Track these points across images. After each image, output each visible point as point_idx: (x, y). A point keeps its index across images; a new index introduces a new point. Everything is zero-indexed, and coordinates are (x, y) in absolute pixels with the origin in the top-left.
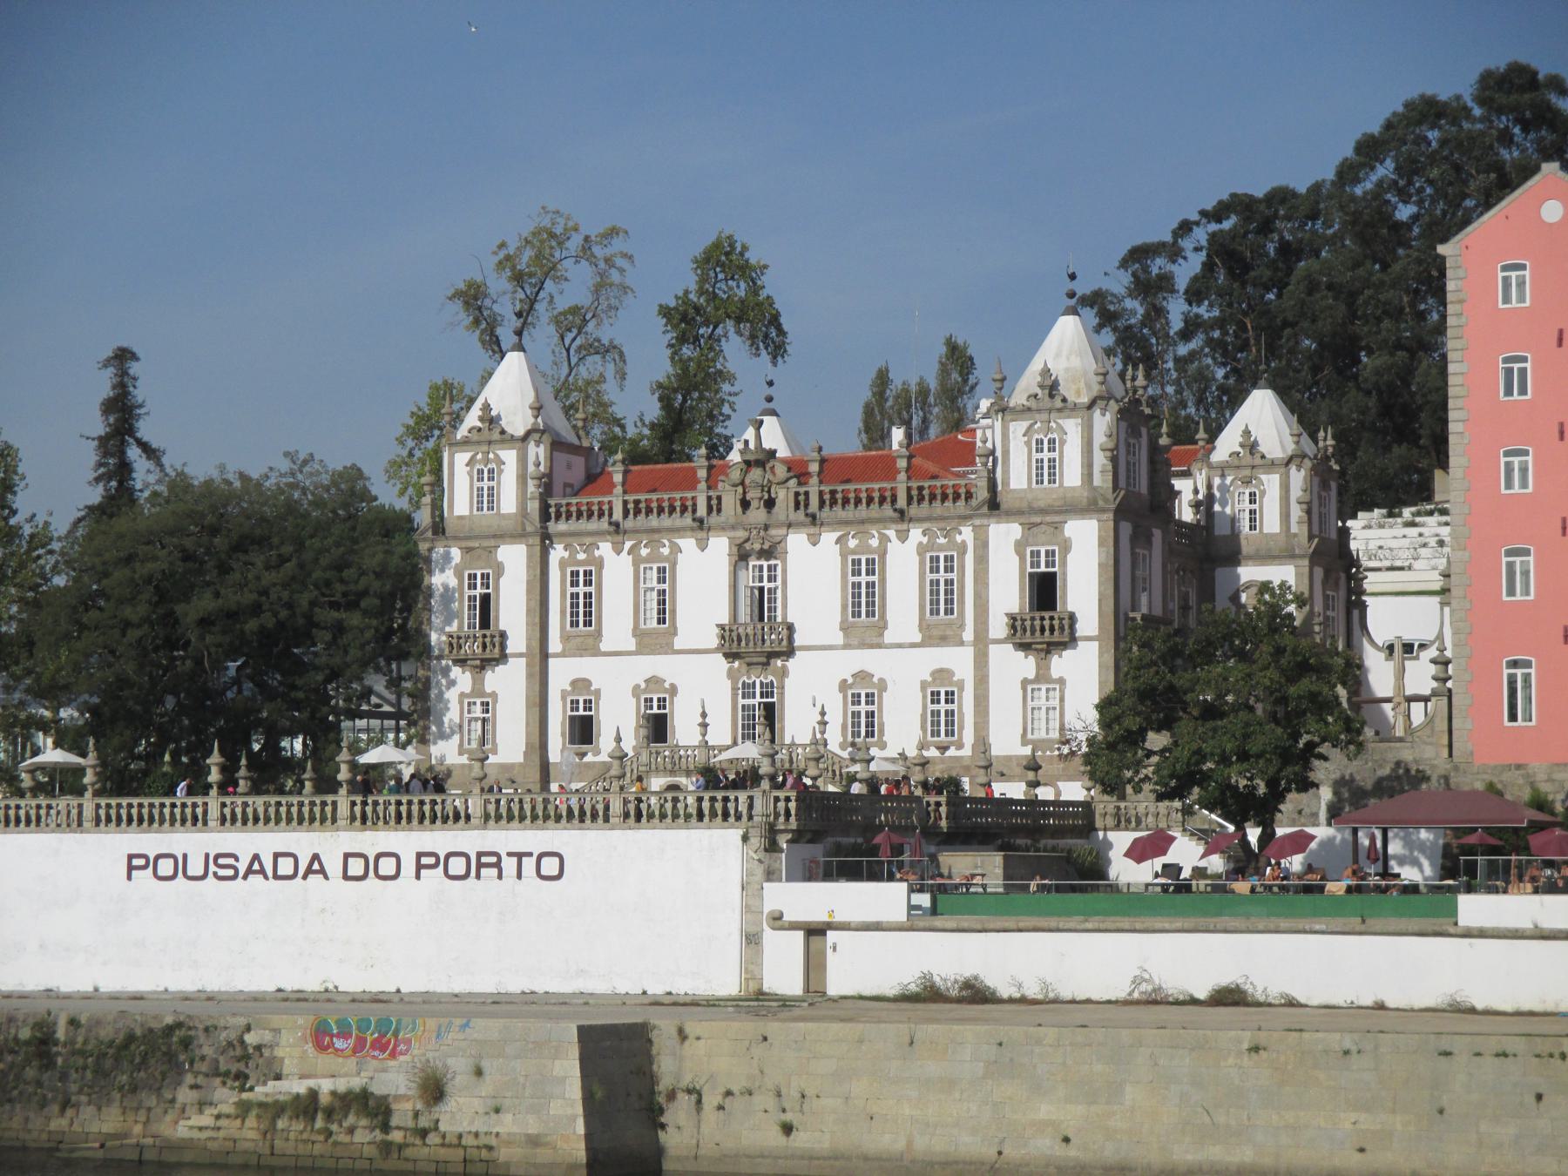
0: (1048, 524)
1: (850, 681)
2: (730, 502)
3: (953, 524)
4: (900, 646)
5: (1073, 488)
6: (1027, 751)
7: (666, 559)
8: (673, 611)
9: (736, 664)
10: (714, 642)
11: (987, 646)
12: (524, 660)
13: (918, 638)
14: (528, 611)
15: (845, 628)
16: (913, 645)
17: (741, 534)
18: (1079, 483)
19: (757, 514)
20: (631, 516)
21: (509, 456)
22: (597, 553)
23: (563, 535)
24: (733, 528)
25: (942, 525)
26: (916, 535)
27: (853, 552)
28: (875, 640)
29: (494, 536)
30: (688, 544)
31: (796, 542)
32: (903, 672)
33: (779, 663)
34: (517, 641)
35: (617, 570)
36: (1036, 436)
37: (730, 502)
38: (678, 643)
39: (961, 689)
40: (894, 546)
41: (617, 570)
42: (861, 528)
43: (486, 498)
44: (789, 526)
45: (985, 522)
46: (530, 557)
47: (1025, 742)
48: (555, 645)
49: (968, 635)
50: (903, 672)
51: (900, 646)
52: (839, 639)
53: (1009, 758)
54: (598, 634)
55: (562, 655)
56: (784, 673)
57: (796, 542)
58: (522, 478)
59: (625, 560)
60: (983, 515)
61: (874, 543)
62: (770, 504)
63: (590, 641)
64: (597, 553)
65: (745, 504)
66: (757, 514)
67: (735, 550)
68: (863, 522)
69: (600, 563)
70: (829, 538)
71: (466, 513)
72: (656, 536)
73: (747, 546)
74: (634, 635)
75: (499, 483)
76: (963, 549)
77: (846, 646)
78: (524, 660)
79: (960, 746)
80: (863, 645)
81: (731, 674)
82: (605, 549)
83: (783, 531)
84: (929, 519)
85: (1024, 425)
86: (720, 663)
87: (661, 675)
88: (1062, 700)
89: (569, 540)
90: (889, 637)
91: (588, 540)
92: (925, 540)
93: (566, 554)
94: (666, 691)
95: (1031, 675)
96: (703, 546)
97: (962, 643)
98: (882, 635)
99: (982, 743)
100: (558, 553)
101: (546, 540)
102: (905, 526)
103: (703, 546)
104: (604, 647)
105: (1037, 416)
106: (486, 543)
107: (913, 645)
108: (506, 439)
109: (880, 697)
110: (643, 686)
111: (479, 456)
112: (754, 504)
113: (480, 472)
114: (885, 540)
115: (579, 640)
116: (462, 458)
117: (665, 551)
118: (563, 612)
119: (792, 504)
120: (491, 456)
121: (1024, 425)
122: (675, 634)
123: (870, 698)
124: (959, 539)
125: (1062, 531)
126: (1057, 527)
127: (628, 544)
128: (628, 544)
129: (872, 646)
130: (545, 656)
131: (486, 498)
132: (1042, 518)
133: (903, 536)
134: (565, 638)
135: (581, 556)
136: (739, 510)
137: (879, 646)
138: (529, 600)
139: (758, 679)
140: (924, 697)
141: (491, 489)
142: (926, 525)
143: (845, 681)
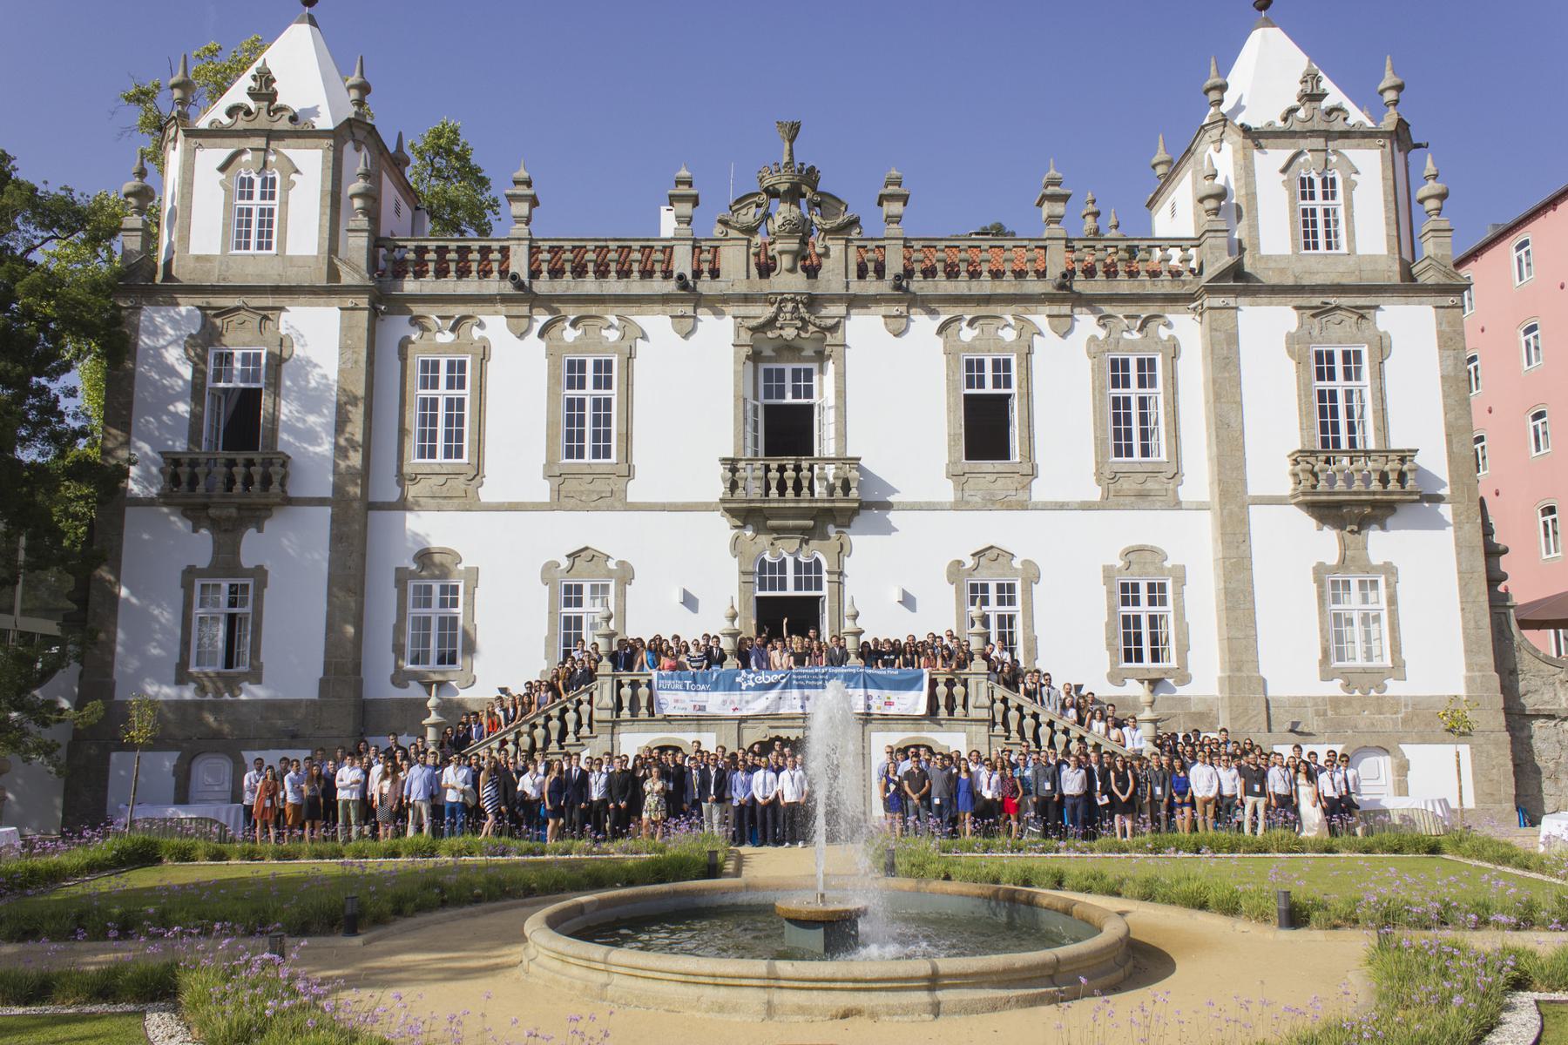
2: (734, 259)
3: (1152, 309)
4: (1062, 506)
5: (1373, 258)
6: (1335, 688)
7: (615, 348)
8: (627, 437)
11: (1244, 507)
12: (328, 510)
13: (1096, 494)
16: (1086, 506)
21: (310, 161)
24: (746, 299)
25: (1132, 309)
29: (276, 290)
30: (656, 323)
35: (516, 370)
37: (734, 259)
39: (1181, 581)
43: (252, 226)
45: (1231, 301)
46: (346, 330)
47: (1327, 674)
51: (1062, 506)
52: (946, 491)
53: (1299, 703)
57: (864, 330)
61: (1009, 335)
70: (923, 325)
71: (215, 249)
75: (285, 203)
76: (1174, 353)
77: (960, 505)
82: (494, 326)
86: (721, 527)
88: (1392, 600)
90: (1040, 491)
91: (458, 311)
92: (1102, 334)
95: (1333, 559)
97: (1177, 505)
98: (1027, 487)
104: (487, 494)
107: (1086, 506)
108: (300, 130)
109: (1028, 592)
111: (247, 157)
114: (1027, 332)
116: (211, 157)
122: (629, 474)
123: (1006, 594)
129: (1009, 507)
131: (252, 226)
132: (1331, 298)
137: (1023, 506)
141: (266, 213)
143: (960, 563)
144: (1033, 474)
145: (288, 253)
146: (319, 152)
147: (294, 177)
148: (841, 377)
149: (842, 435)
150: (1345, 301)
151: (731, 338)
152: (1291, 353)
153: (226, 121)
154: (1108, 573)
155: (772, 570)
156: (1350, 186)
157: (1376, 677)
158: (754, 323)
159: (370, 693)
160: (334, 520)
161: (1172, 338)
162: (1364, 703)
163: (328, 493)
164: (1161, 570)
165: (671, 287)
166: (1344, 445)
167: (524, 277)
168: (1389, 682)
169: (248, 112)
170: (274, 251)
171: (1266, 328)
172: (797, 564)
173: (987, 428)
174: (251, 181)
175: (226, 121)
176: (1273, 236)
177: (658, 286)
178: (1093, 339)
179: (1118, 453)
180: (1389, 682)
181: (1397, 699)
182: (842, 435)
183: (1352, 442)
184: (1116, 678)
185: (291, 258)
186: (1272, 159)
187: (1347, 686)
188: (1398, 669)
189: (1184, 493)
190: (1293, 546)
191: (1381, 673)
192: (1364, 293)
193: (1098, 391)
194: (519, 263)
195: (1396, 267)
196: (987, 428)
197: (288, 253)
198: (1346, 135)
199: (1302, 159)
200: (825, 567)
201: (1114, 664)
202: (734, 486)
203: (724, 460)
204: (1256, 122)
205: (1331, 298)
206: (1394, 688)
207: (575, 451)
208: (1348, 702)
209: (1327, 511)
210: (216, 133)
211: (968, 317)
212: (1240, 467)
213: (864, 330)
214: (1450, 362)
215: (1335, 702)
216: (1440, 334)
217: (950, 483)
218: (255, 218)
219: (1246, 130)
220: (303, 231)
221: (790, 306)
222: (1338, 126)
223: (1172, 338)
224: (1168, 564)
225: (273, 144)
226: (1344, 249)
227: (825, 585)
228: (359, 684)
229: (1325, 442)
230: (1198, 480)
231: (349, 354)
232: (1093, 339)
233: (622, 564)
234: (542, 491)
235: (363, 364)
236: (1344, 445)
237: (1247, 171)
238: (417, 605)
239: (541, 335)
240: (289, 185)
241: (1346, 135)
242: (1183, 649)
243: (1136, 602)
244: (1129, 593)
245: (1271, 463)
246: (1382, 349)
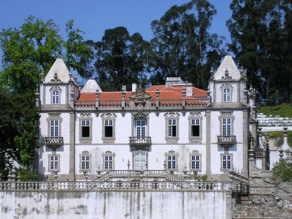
5: (235, 103)
10: (128, 142)
18: (237, 101)
27: (169, 118)
30: (119, 115)
31: (152, 116)
40: (181, 117)
48: (77, 141)
49: (204, 141)
53: (217, 175)
57: (152, 116)
58: (67, 94)
70: (162, 114)
77: (166, 144)
97: (201, 144)
98: (177, 141)
104: (92, 142)
123: (174, 158)
125: (232, 114)
129: (174, 144)
134: (81, 140)
137: (177, 144)
140: (190, 158)
145: (61, 104)
156: (232, 91)
158: (134, 114)
170: (59, 103)
173: (173, 131)
182: (148, 133)
189: (202, 142)
192: (231, 110)
196: (173, 131)
197: (61, 104)
208: (224, 175)
214: (245, 121)
215: (222, 175)
220: (63, 100)
224: (199, 153)
225: (57, 86)
239: (101, 117)
241: (232, 82)
242: (201, 167)
244: (193, 158)
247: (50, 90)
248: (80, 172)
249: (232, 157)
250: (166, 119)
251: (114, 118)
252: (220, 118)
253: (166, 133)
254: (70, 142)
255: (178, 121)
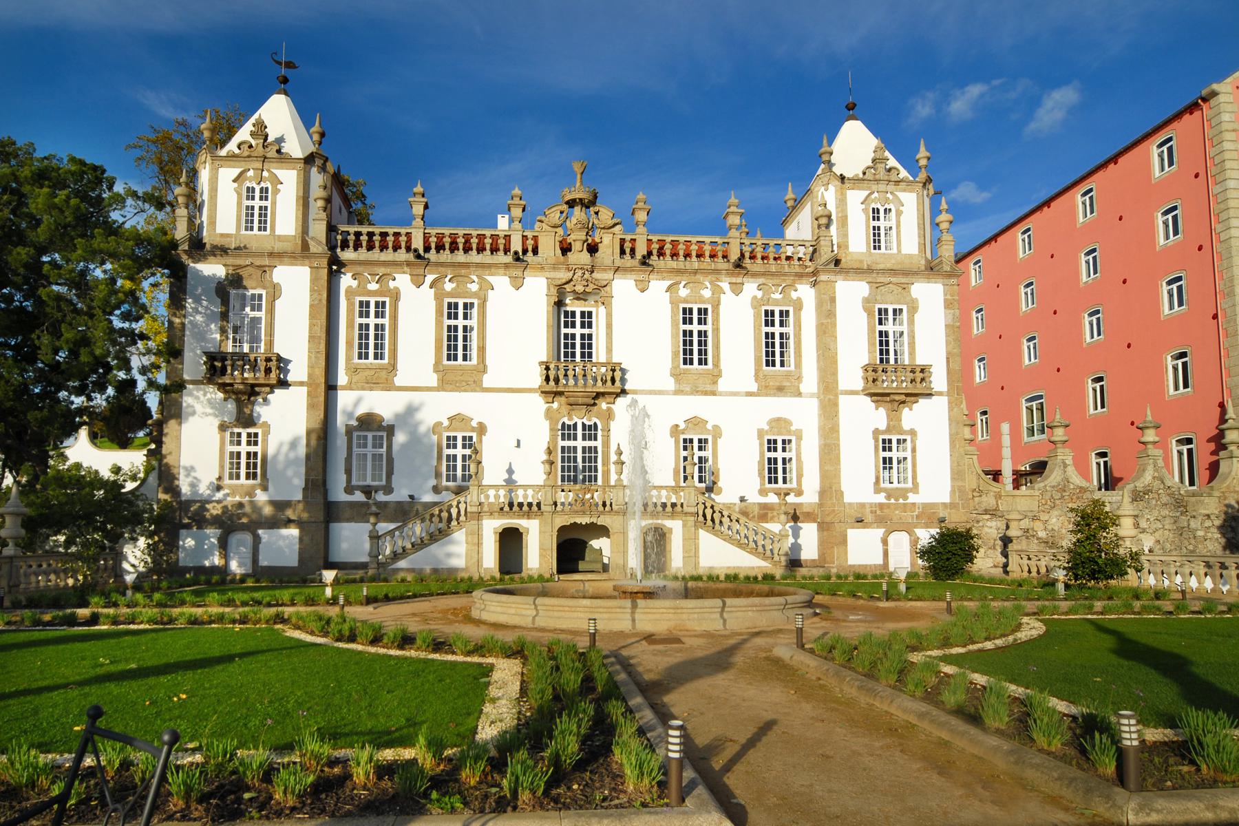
0: (897, 284)
1: (682, 426)
3: (789, 280)
5: (911, 256)
6: (881, 498)
7: (475, 295)
8: (482, 349)
9: (555, 405)
11: (836, 396)
12: (305, 389)
13: (754, 387)
14: (312, 338)
15: (676, 375)
16: (749, 394)
17: (563, 275)
18: (916, 252)
19: (579, 256)
20: (433, 251)
21: (289, 178)
22: (392, 284)
23: (353, 262)
24: (555, 267)
25: (776, 281)
26: (751, 288)
27: (685, 301)
28: (709, 388)
29: (271, 255)
30: (500, 282)
32: (738, 421)
33: (604, 406)
34: (298, 371)
35: (417, 307)
36: (873, 205)
37: (549, 247)
38: (488, 381)
39: (799, 438)
40: (727, 298)
41: (417, 307)
42: (693, 278)
44: (617, 270)
45: (833, 278)
46: (314, 281)
47: (878, 490)
50: (738, 421)
52: (670, 384)
53: (862, 505)
54: (393, 367)
55: (349, 387)
56: (610, 415)
57: (623, 288)
58: (305, 201)
59: (427, 293)
60: (829, 271)
61: (707, 293)
62: (593, 249)
63: (383, 374)
64: (392, 284)
65: (566, 249)
66: (579, 256)
67: (554, 291)
68: (695, 272)
69: (396, 296)
70: (658, 286)
71: (232, 230)
72: (463, 272)
73: (568, 288)
74: (436, 370)
75: (274, 203)
76: (799, 305)
78: (305, 389)
79: (799, 493)
80: (696, 391)
81: (549, 414)
82: (402, 281)
83: (609, 275)
84: (764, 274)
85: (863, 194)
86: (538, 404)
87: (467, 412)
88: (914, 450)
89: (359, 269)
90: (722, 385)
91: (381, 270)
92: (759, 294)
93: (355, 284)
94: (473, 429)
95: (883, 427)
96: (517, 284)
97: (799, 394)
98: (715, 383)
99: (830, 487)
100: (346, 281)
101: (335, 267)
102: (739, 280)
103: (517, 284)
104: (398, 381)
105: (874, 187)
106: (258, 262)
107: (749, 394)
110: (446, 423)
111: (251, 173)
112: (577, 246)
113: (250, 190)
114: (718, 291)
115: (367, 373)
116: (227, 174)
117: (474, 287)
118: (349, 344)
119: (618, 251)
120: (265, 174)
121: (863, 194)
122: (485, 371)
124: (794, 295)
126: (905, 288)
127: (430, 278)
128: (430, 278)
129: (706, 393)
130: (331, 387)
133: (737, 289)
134: (353, 370)
135: (373, 286)
136: (559, 252)
137: (714, 393)
138: (312, 326)
139: (579, 419)
140: (761, 445)
142: (762, 280)
144: (719, 375)
145: (277, 233)
146: (295, 172)
147: (279, 186)
148: (609, 316)
149: (609, 350)
150: (894, 280)
151: (545, 291)
152: (865, 309)
153: (237, 151)
154: (761, 433)
155: (569, 429)
156: (899, 213)
157: (903, 493)
158: (559, 283)
159: (332, 498)
160: (309, 395)
161: (799, 299)
162: (897, 506)
163: (305, 379)
164: (789, 433)
165: (509, 259)
166: (892, 362)
167: (421, 252)
168: (910, 495)
169: (251, 146)
170: (268, 232)
171: (851, 294)
172: (584, 425)
173: (694, 348)
174: (253, 189)
175: (237, 151)
176: (858, 243)
177: (501, 258)
178: (755, 298)
179: (767, 365)
180: (910, 495)
181: (914, 504)
182: (609, 350)
183: (896, 360)
184: (763, 492)
185: (279, 236)
186: (855, 197)
187: (888, 497)
188: (915, 488)
189: (803, 388)
190: (861, 418)
191: (906, 491)
192: (905, 273)
193: (757, 329)
194: (418, 243)
195: (923, 262)
196: (694, 348)
197: (277, 233)
198: (897, 182)
199: (873, 196)
200: (600, 427)
201: (762, 484)
202: (547, 379)
203: (541, 363)
204: (848, 174)
205: (890, 278)
206: (912, 498)
207: (452, 357)
208: (888, 506)
209: (879, 397)
210: (232, 157)
211: (683, 283)
212: (835, 373)
213: (623, 288)
214: (950, 316)
215: (881, 506)
216: (946, 301)
217: (672, 380)
218: (256, 212)
219: (842, 178)
220: (286, 221)
221: (579, 273)
222: (893, 177)
223: (799, 299)
224: (793, 428)
226: (895, 251)
227: (599, 437)
228: (325, 493)
229: (881, 360)
230: (810, 380)
231: (316, 295)
232: (755, 298)
233: (480, 424)
234: (433, 380)
235: (325, 302)
236: (892, 362)
237: (842, 202)
238: (359, 446)
240: (276, 191)
243: (775, 450)
244: (772, 445)
245: (851, 374)
246: (913, 309)
247: (234, 181)
248: (349, 489)
249: (913, 441)
250: (671, 303)
251: (482, 293)
252: (867, 303)
253: (675, 354)
254: (310, 376)
255: (718, 314)
